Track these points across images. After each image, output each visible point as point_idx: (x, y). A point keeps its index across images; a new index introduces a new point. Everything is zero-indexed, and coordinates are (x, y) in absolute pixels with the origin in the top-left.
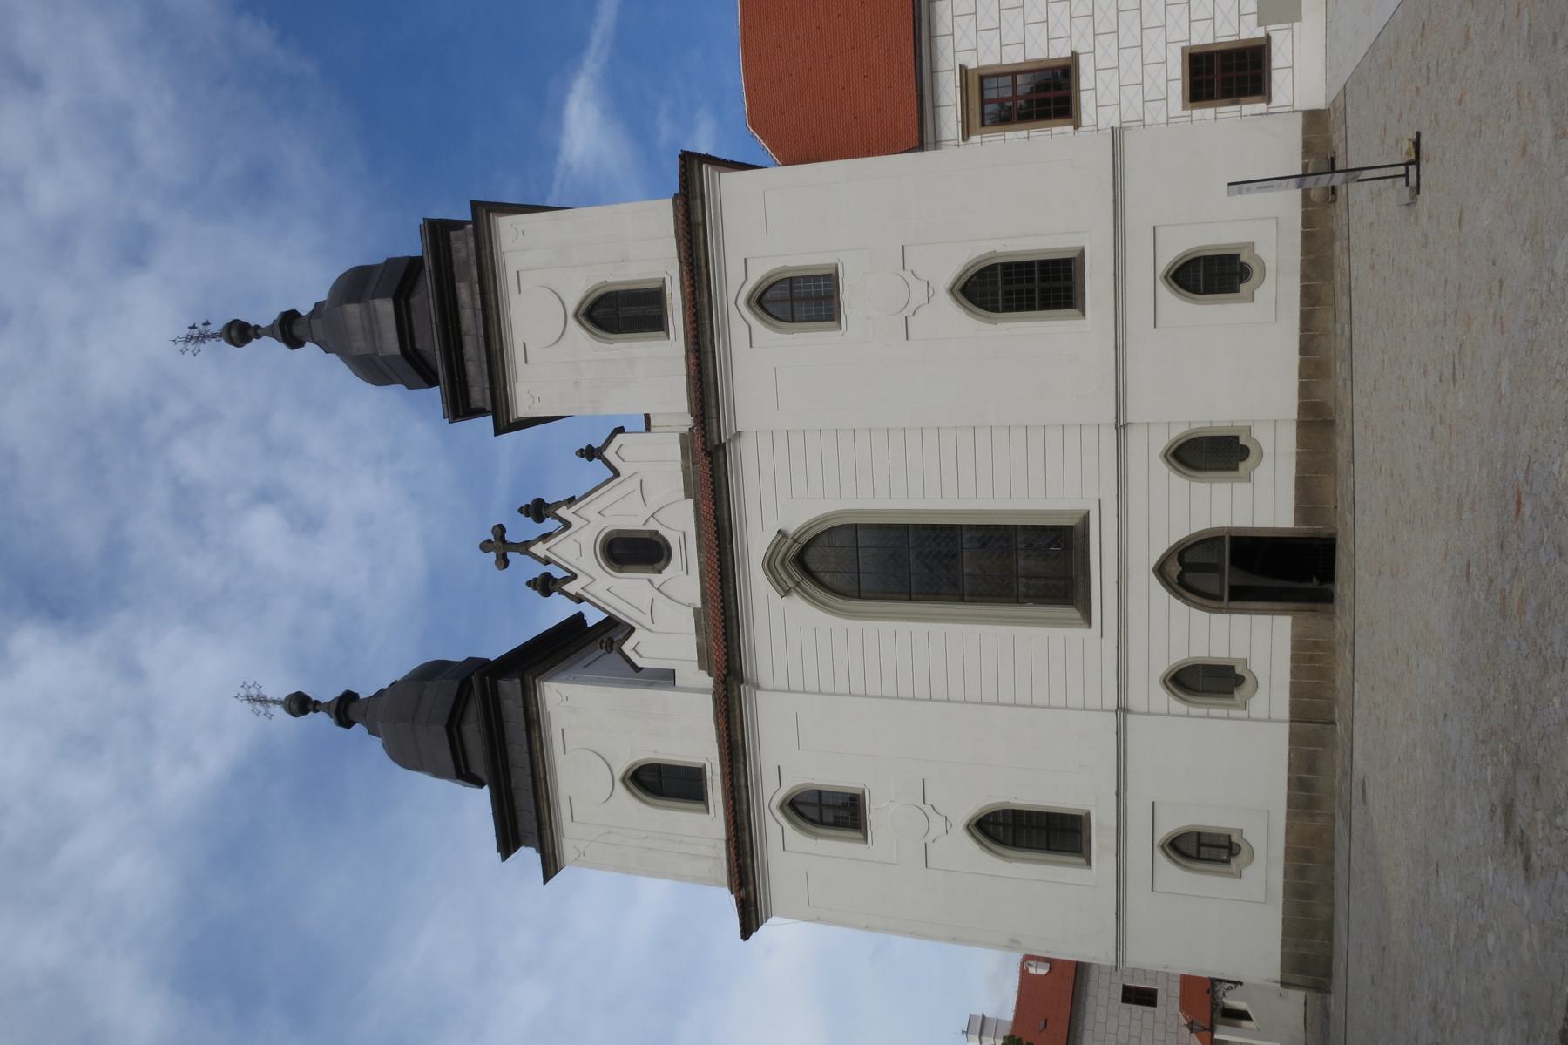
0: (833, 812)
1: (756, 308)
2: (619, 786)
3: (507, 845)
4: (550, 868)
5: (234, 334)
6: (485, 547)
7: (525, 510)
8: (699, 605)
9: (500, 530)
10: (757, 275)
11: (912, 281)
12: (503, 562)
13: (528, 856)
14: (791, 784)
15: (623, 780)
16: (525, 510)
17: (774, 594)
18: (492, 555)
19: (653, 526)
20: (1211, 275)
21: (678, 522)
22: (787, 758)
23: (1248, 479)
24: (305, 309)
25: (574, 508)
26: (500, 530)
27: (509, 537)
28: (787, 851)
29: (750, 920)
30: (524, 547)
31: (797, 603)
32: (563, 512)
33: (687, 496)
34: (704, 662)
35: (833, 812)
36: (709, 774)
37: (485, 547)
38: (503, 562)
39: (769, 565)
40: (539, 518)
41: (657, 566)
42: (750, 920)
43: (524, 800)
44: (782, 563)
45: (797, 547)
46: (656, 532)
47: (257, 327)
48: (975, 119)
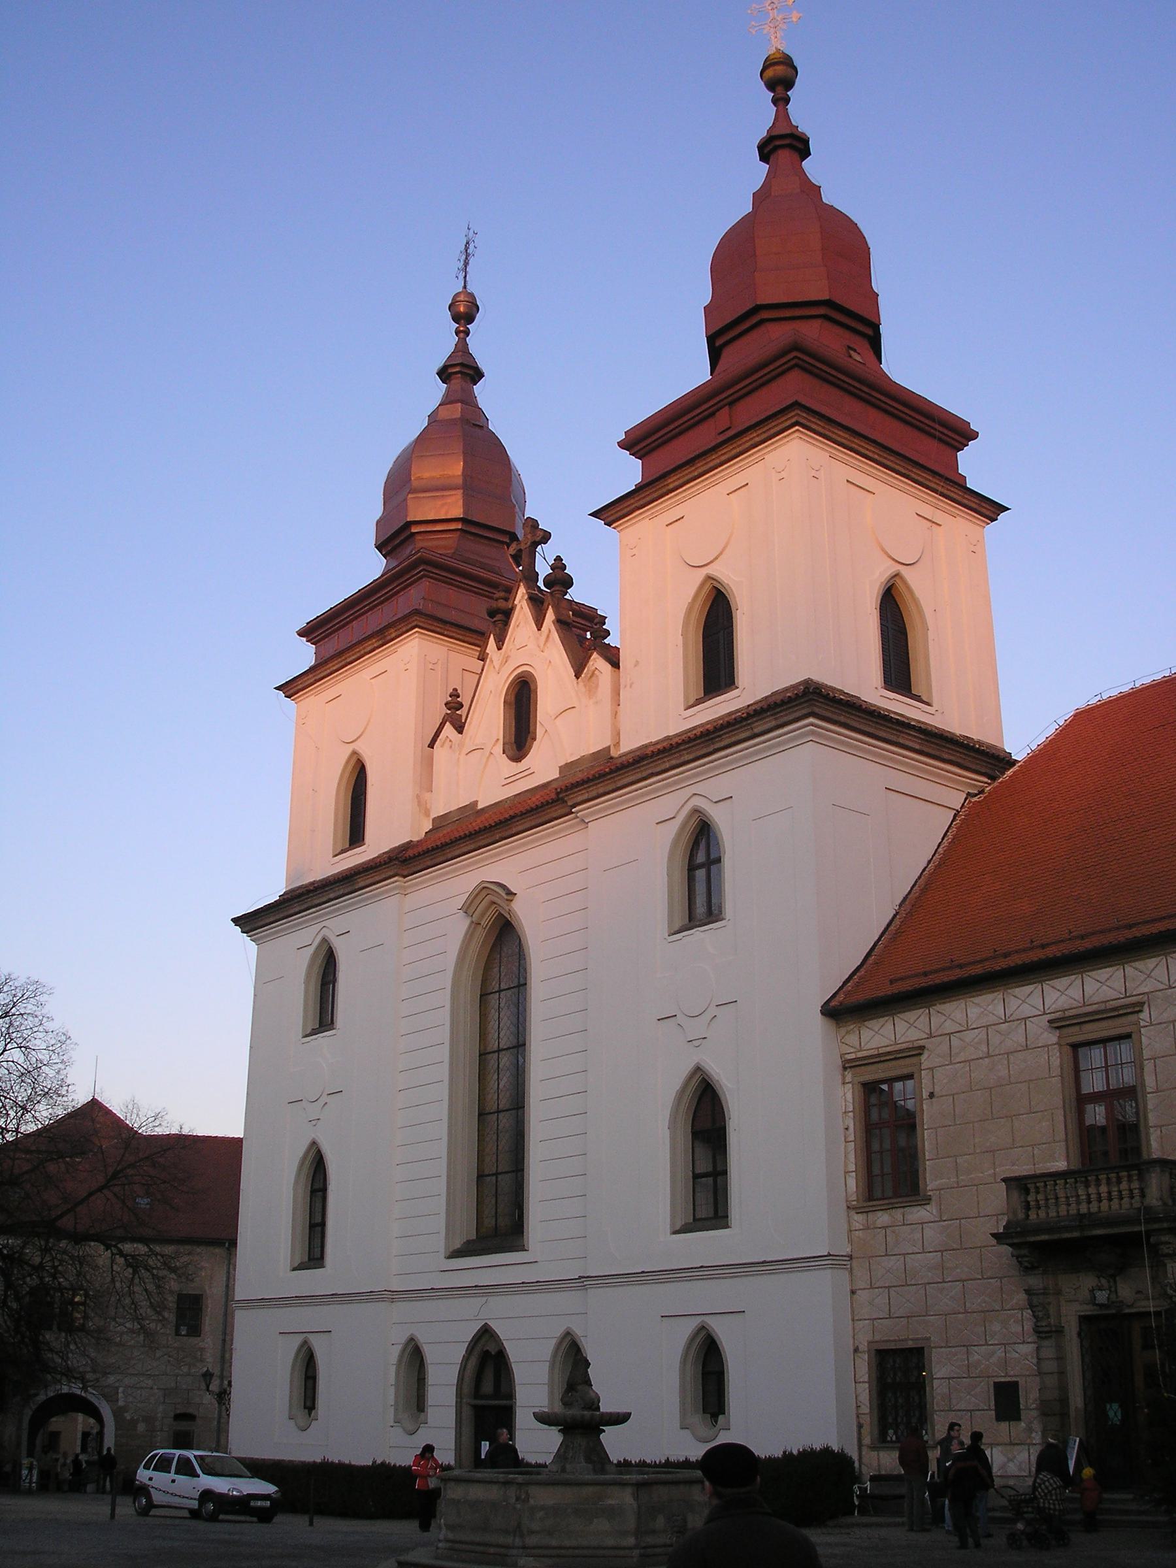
3: (310, 632)
5: (780, 70)
8: (480, 807)
11: (707, 1016)
17: (461, 901)
24: (805, 164)
29: (249, 923)
31: (459, 926)
34: (440, 822)
39: (484, 889)
43: (357, 629)
46: (534, 739)
47: (787, 100)
48: (871, 1074)
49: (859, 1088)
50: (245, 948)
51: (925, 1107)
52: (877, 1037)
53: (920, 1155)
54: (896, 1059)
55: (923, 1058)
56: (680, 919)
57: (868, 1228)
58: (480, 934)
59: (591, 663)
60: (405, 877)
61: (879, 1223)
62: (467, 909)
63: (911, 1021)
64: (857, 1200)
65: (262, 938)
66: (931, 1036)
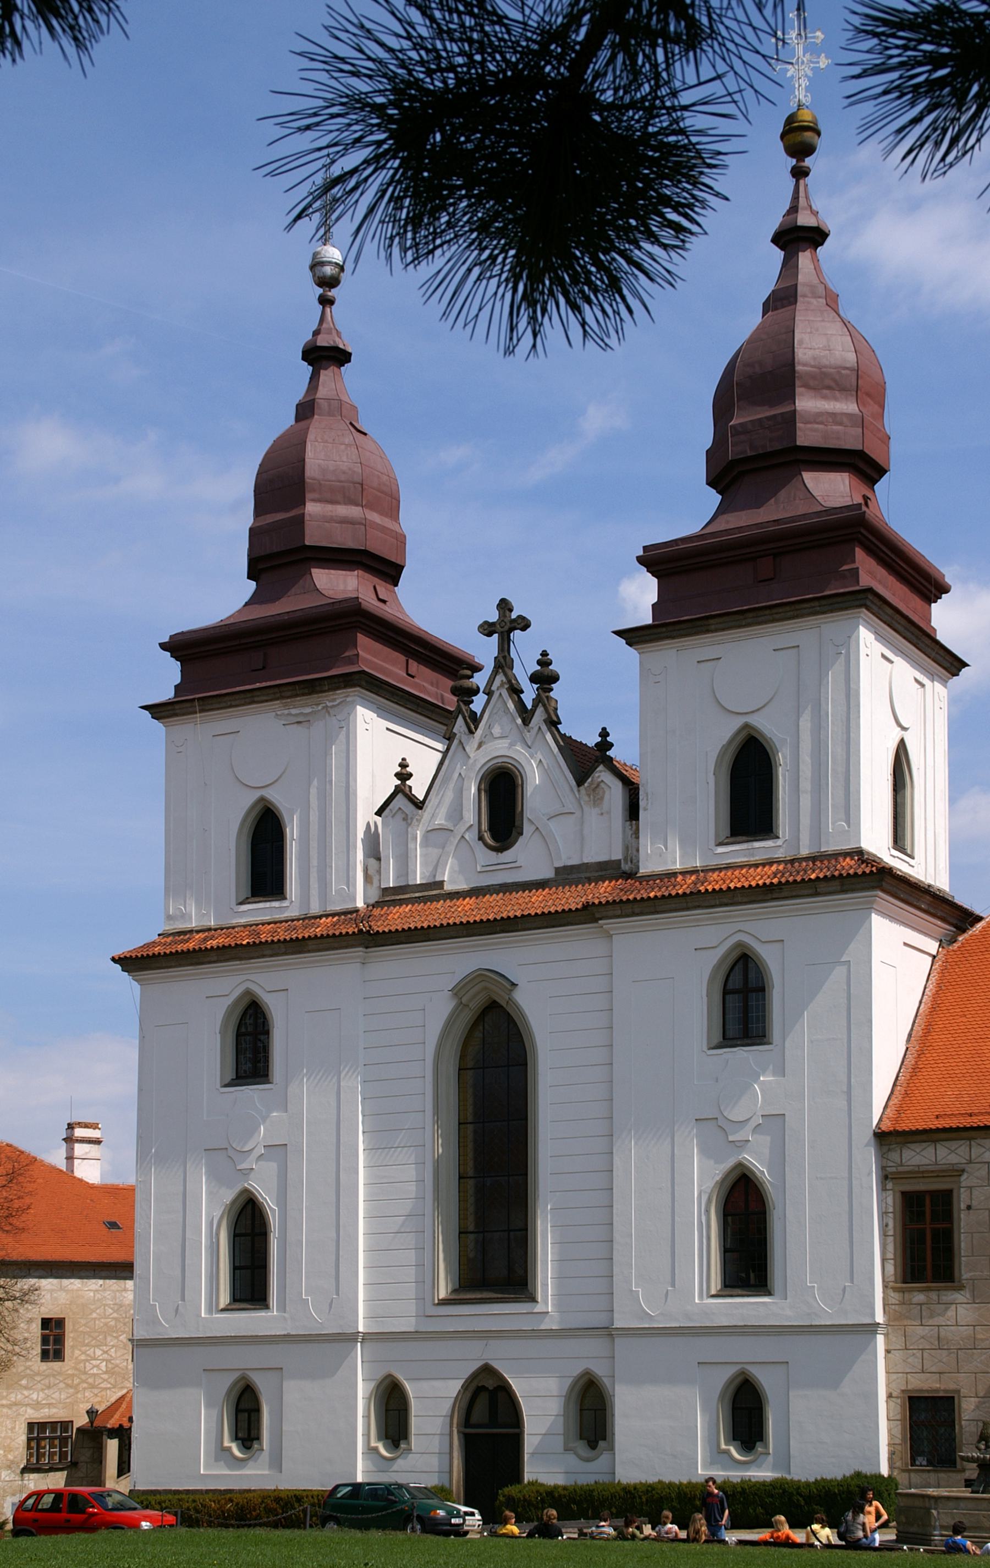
0: (251, 1049)
1: (735, 955)
2: (257, 795)
4: (158, 711)
6: (504, 606)
7: (544, 661)
9: (524, 624)
10: (768, 955)
12: (487, 629)
13: (166, 677)
14: (274, 1006)
15: (262, 799)
16: (544, 661)
18: (494, 617)
19: (527, 829)
20: (746, 1414)
21: (529, 858)
22: (296, 996)
23: (567, 1449)
25: (544, 728)
26: (524, 624)
27: (517, 635)
28: (208, 999)
29: (130, 963)
30: (503, 663)
32: (539, 715)
33: (557, 870)
35: (251, 1049)
36: (276, 904)
37: (504, 606)
38: (487, 629)
39: (484, 977)
40: (534, 678)
41: (487, 836)
42: (130, 963)
44: (486, 988)
45: (504, 1004)
49: (898, 1195)
50: (127, 987)
51: (962, 1216)
52: (918, 1157)
53: (956, 1252)
54: (938, 1176)
55: (963, 1178)
56: (718, 1037)
57: (904, 1304)
58: (467, 1017)
59: (596, 774)
60: (367, 948)
61: (915, 1300)
62: (457, 991)
63: (953, 1148)
64: (896, 1282)
65: (145, 980)
66: (970, 1162)
